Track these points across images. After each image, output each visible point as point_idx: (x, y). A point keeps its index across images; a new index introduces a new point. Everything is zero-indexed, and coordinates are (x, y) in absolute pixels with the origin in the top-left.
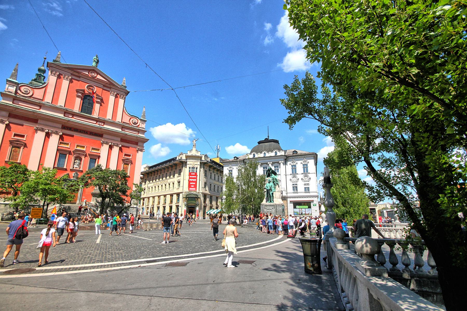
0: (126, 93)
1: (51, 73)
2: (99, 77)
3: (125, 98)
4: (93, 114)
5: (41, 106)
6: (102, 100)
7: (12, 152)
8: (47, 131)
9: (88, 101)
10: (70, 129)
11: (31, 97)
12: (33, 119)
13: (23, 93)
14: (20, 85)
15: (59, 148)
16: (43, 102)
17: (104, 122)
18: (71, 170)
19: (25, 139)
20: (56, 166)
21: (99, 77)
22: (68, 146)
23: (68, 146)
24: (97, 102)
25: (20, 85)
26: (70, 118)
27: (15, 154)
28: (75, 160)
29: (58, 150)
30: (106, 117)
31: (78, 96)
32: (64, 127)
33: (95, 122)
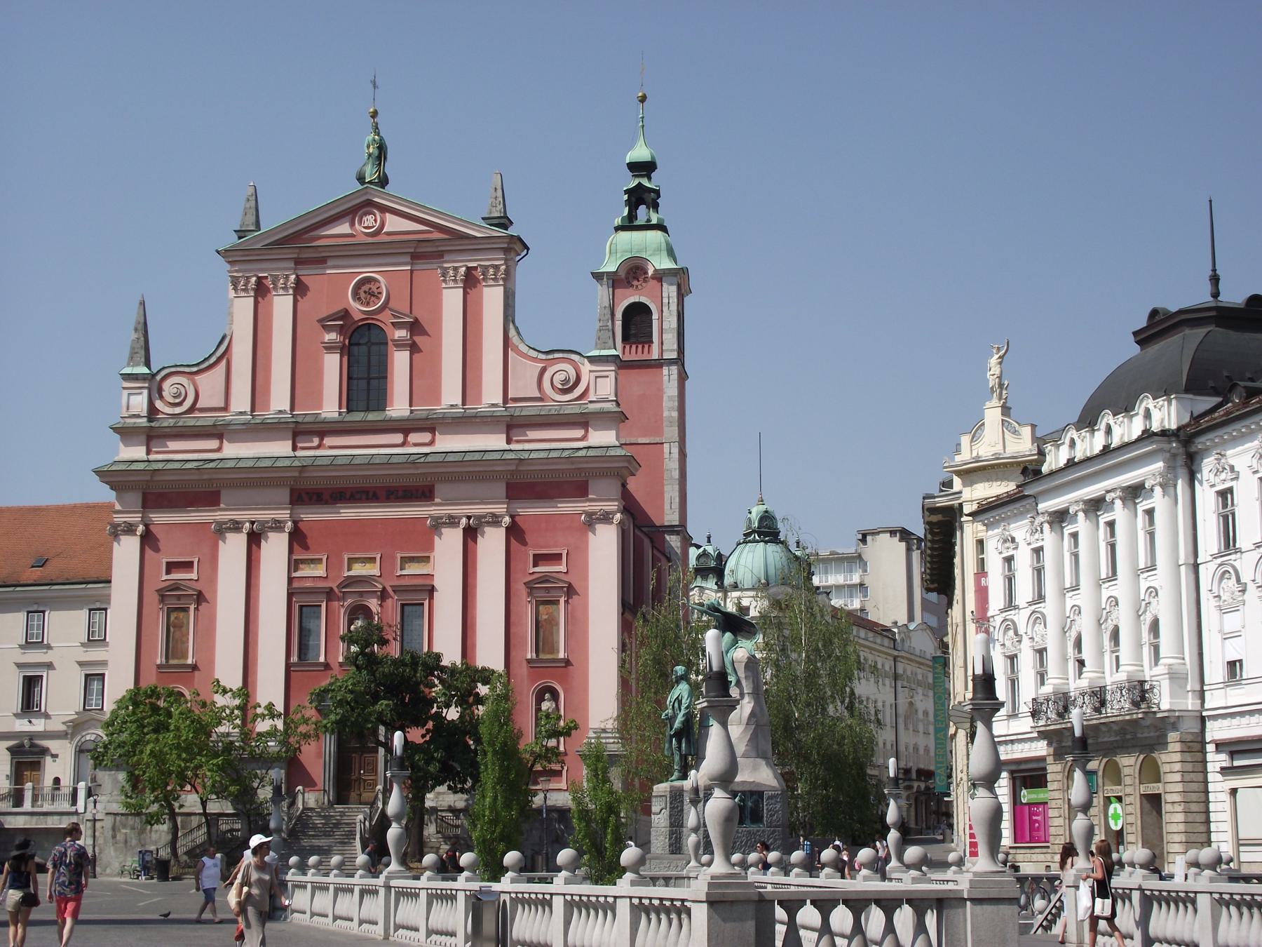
1: (235, 289)
2: (394, 224)
5: (218, 432)
6: (415, 327)
9: (363, 349)
11: (192, 409)
12: (200, 490)
14: (158, 378)
15: (296, 584)
16: (228, 416)
17: (431, 425)
22: (320, 571)
23: (320, 571)
24: (400, 345)
25: (158, 378)
26: (309, 452)
27: (178, 634)
29: (290, 595)
30: (438, 400)
31: (330, 348)
33: (398, 438)
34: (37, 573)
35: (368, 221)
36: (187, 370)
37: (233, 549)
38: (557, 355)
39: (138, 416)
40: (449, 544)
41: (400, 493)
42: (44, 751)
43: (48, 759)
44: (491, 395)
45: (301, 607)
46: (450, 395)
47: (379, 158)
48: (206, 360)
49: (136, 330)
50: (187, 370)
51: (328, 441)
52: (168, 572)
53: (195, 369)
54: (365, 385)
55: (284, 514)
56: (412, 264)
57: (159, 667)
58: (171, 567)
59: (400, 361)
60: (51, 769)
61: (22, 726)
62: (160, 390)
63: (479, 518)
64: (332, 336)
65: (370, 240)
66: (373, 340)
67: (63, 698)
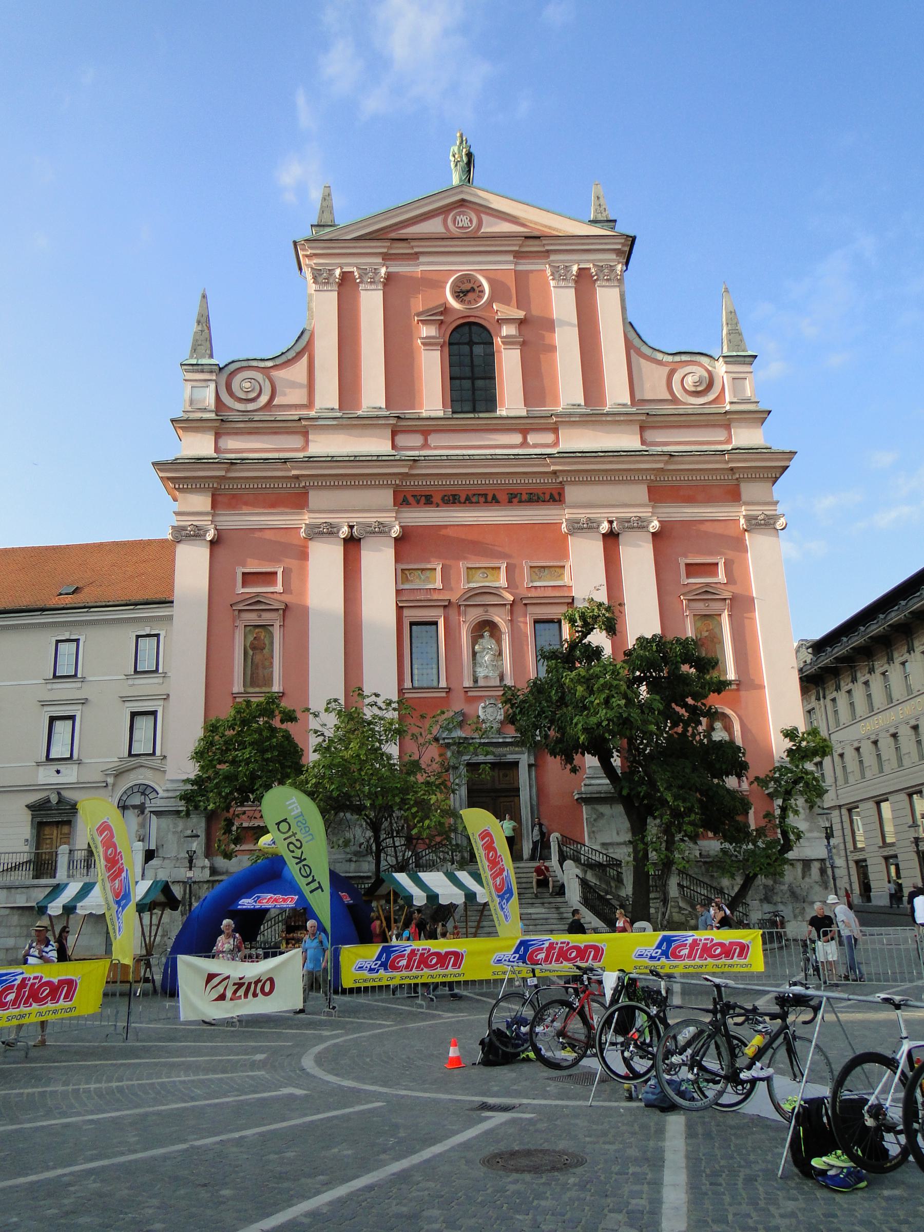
0: (618, 252)
3: (621, 281)
4: (503, 405)
7: (251, 652)
8: (345, 529)
10: (427, 500)
13: (240, 400)
16: (312, 414)
18: (466, 690)
20: (408, 684)
24: (509, 342)
27: (258, 658)
28: (474, 641)
29: (400, 609)
31: (428, 343)
32: (403, 500)
33: (517, 439)
35: (463, 220)
36: (262, 364)
38: (684, 358)
39: (204, 410)
41: (525, 497)
44: (616, 393)
45: (412, 624)
47: (469, 164)
48: (283, 353)
49: (199, 322)
50: (262, 364)
52: (243, 586)
53: (270, 364)
54: (472, 383)
55: (388, 517)
56: (516, 264)
58: (248, 578)
60: (85, 831)
61: (46, 776)
63: (621, 521)
66: (476, 339)
67: (102, 740)
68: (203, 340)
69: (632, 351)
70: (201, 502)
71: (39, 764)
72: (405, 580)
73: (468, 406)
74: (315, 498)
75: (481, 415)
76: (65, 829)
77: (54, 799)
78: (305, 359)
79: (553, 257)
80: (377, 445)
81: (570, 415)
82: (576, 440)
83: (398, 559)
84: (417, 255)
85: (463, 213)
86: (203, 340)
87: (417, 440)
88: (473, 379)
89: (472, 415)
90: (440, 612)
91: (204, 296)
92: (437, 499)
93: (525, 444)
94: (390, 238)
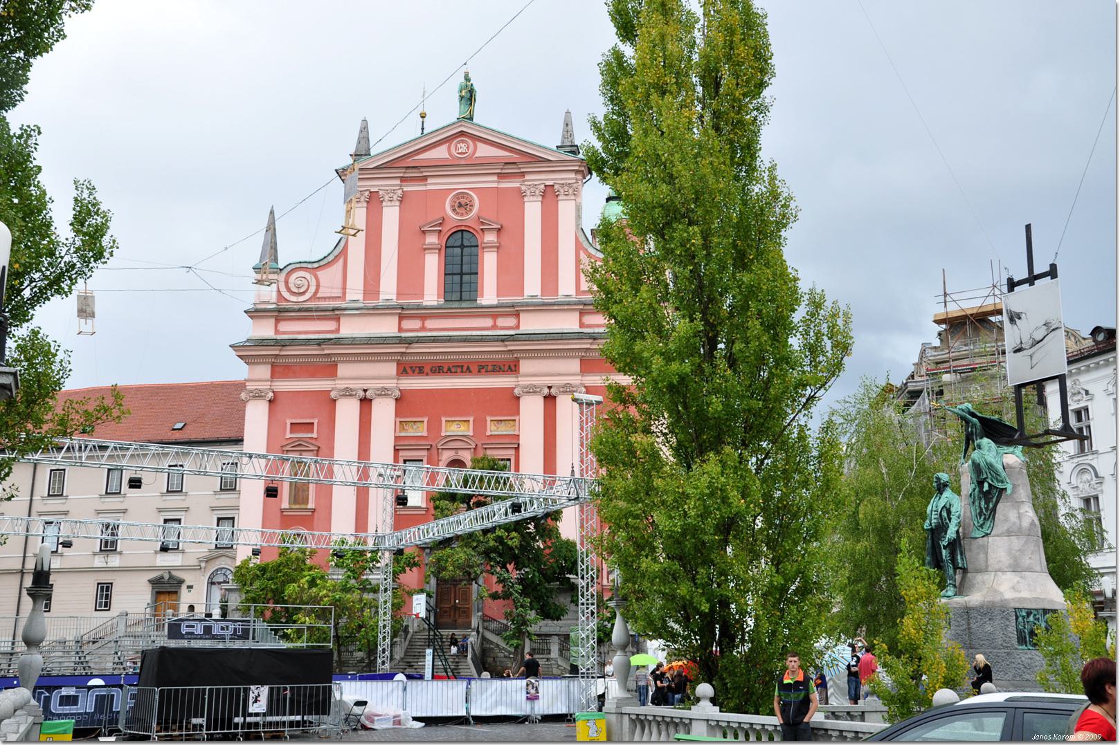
2: (484, 151)
5: (334, 314)
8: (362, 394)
13: (294, 294)
14: (286, 271)
17: (515, 311)
19: (315, 435)
21: (484, 151)
22: (422, 430)
24: (490, 246)
29: (396, 451)
33: (488, 322)
34: (177, 436)
36: (310, 266)
37: (348, 412)
40: (531, 410)
41: (490, 368)
42: (181, 582)
43: (184, 587)
46: (532, 287)
50: (310, 266)
51: (430, 324)
53: (316, 265)
54: (461, 280)
57: (282, 511)
59: (489, 262)
62: (286, 282)
63: (559, 387)
64: (432, 239)
65: (463, 162)
68: (271, 247)
69: (581, 252)
70: (264, 371)
71: (156, 552)
72: (403, 429)
73: (456, 296)
74: (343, 370)
75: (464, 305)
76: (174, 597)
77: (167, 576)
78: (341, 261)
79: (527, 177)
80: (387, 327)
81: (528, 305)
82: (532, 324)
83: (396, 415)
84: (425, 178)
85: (463, 141)
86: (271, 247)
87: (416, 324)
88: (462, 274)
89: (456, 305)
90: (425, 453)
91: (272, 212)
92: (427, 370)
93: (494, 327)
94: (406, 165)
